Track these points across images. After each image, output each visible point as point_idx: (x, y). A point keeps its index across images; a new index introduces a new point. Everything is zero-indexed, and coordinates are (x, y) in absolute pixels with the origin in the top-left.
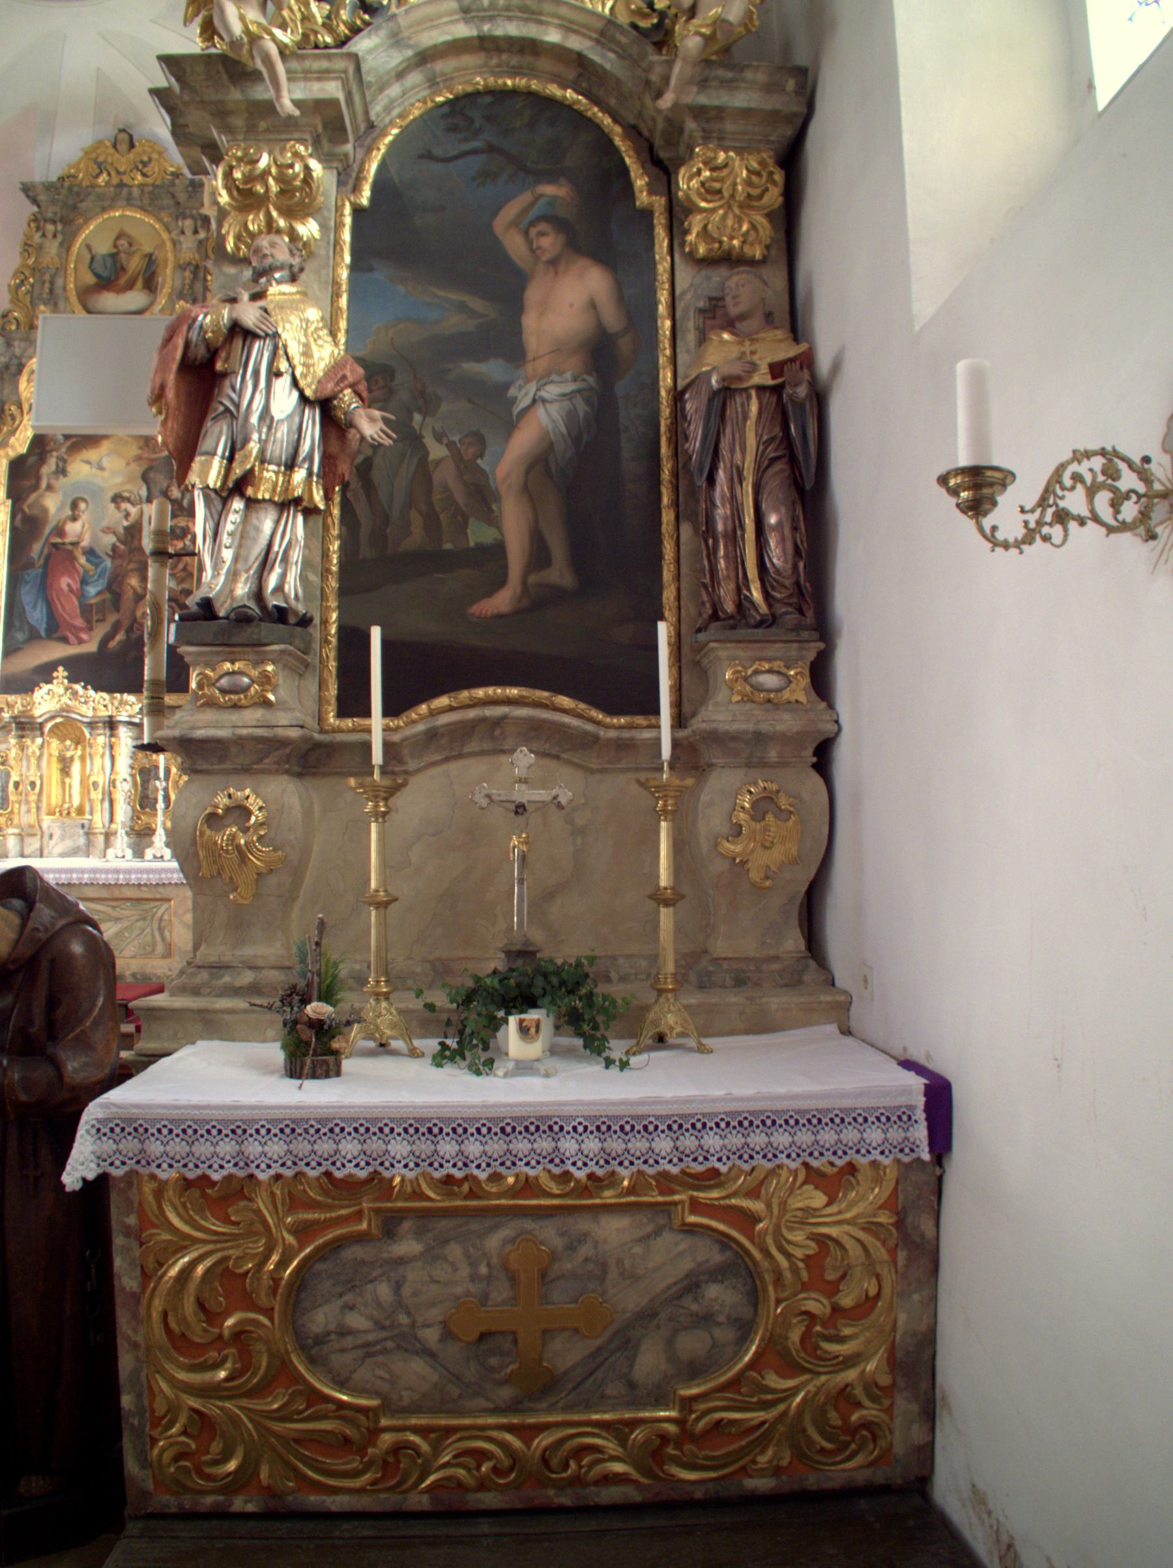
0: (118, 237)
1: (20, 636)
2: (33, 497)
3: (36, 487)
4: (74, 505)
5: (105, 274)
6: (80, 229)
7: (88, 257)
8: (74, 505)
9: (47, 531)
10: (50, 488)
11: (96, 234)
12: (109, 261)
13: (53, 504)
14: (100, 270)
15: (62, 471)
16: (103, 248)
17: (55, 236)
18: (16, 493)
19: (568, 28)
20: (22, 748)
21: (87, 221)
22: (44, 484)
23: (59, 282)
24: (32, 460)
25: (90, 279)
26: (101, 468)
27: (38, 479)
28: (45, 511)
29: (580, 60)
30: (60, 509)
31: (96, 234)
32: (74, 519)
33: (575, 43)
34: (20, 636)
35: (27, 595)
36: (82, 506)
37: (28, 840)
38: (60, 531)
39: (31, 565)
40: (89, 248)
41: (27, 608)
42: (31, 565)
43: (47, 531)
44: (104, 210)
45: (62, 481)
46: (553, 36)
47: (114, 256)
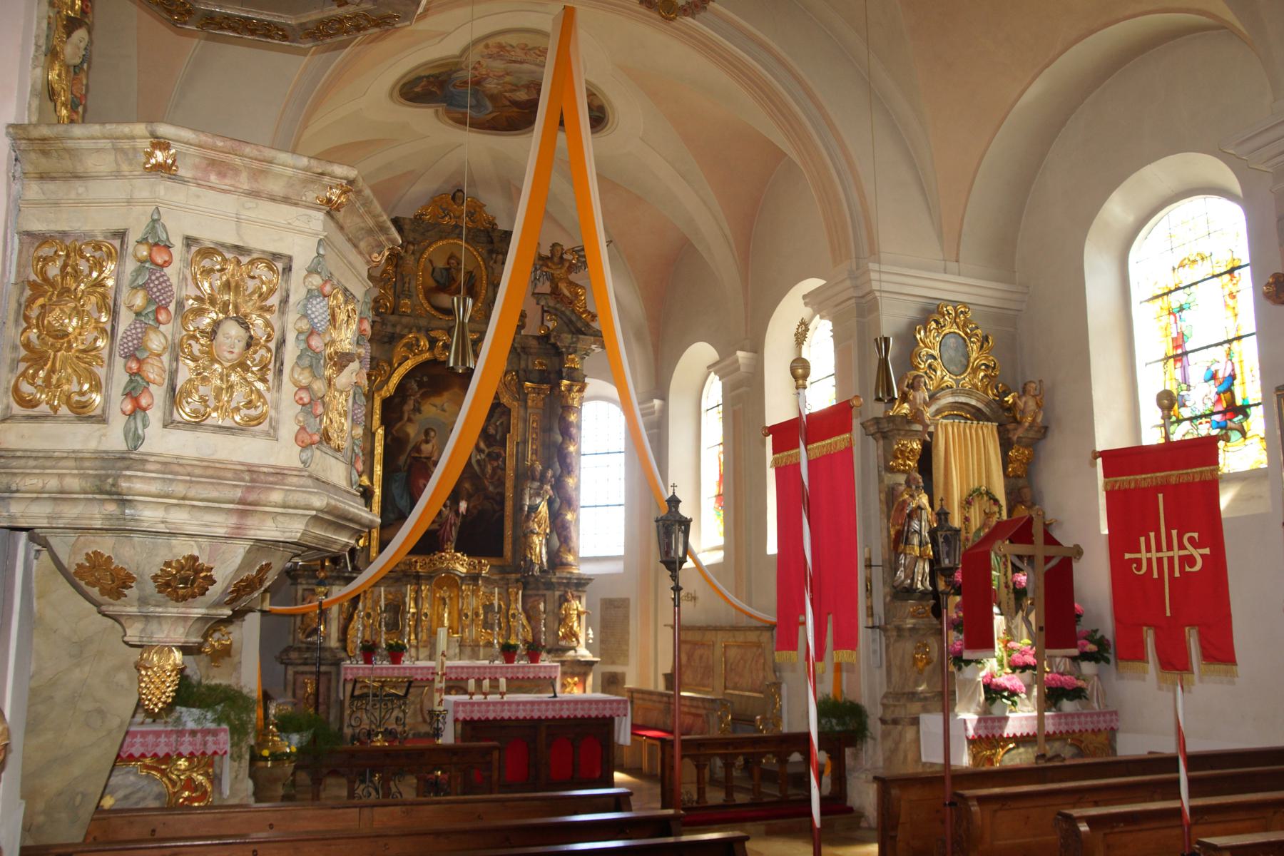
0: (450, 258)
1: (392, 516)
2: (398, 425)
3: (401, 418)
4: (427, 433)
5: (442, 281)
6: (426, 248)
7: (430, 269)
8: (427, 433)
9: (409, 448)
10: (410, 420)
11: (436, 252)
12: (445, 273)
13: (412, 430)
14: (438, 278)
15: (417, 410)
16: (440, 264)
17: (413, 253)
18: (385, 421)
19: (978, 400)
20: (418, 592)
21: (430, 245)
22: (406, 418)
23: (413, 283)
24: (397, 400)
25: (432, 283)
26: (444, 410)
27: (402, 413)
28: (408, 435)
29: (979, 410)
30: (418, 433)
31: (436, 252)
32: (427, 442)
33: (980, 405)
34: (392, 516)
35: (396, 490)
36: (432, 434)
37: (421, 650)
38: (417, 449)
39: (398, 470)
40: (431, 261)
41: (397, 498)
42: (398, 470)
43: (409, 448)
44: (441, 238)
45: (417, 417)
46: (973, 402)
47: (448, 270)
